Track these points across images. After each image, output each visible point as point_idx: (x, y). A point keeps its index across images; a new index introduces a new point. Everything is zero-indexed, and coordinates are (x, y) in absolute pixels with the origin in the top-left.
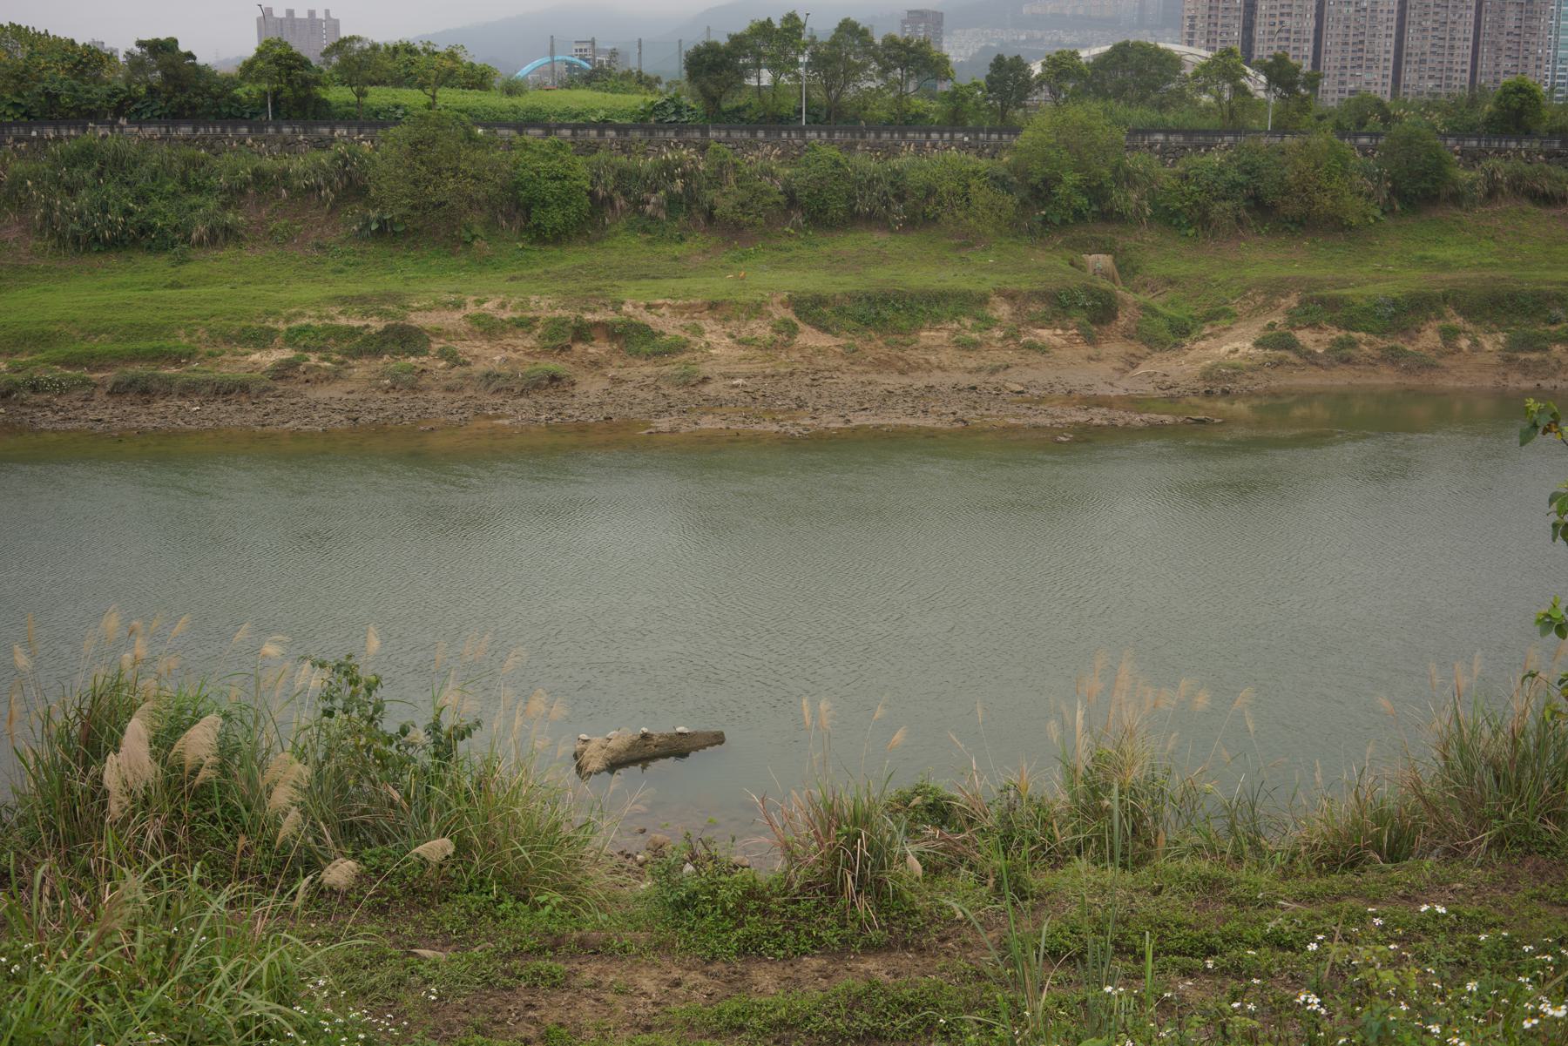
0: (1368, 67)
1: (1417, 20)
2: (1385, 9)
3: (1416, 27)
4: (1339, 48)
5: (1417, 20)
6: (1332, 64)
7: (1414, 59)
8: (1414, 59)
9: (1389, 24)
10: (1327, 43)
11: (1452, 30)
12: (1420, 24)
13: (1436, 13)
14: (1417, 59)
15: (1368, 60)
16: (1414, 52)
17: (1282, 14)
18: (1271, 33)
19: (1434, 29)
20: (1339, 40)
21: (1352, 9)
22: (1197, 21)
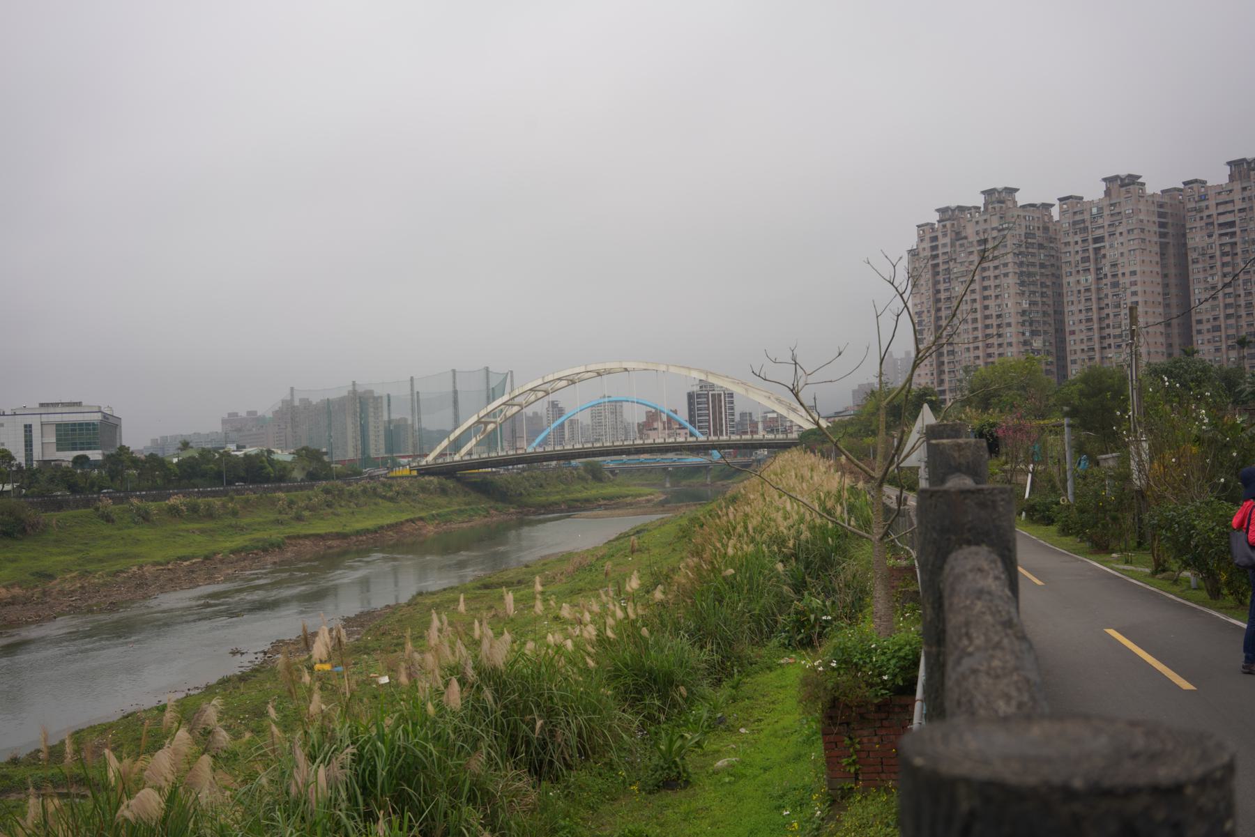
0: (1119, 346)
1: (1201, 276)
2: (1127, 271)
3: (1202, 286)
4: (1083, 327)
5: (1201, 276)
6: (1078, 347)
7: (1205, 327)
8: (1205, 327)
9: (1134, 289)
10: (1070, 322)
11: (1245, 283)
12: (1206, 281)
13: (1224, 265)
14: (1209, 326)
15: (1115, 337)
16: (1204, 317)
17: (985, 298)
18: (975, 320)
19: (1225, 286)
20: (1082, 316)
21: (1091, 278)
22: (925, 317)
